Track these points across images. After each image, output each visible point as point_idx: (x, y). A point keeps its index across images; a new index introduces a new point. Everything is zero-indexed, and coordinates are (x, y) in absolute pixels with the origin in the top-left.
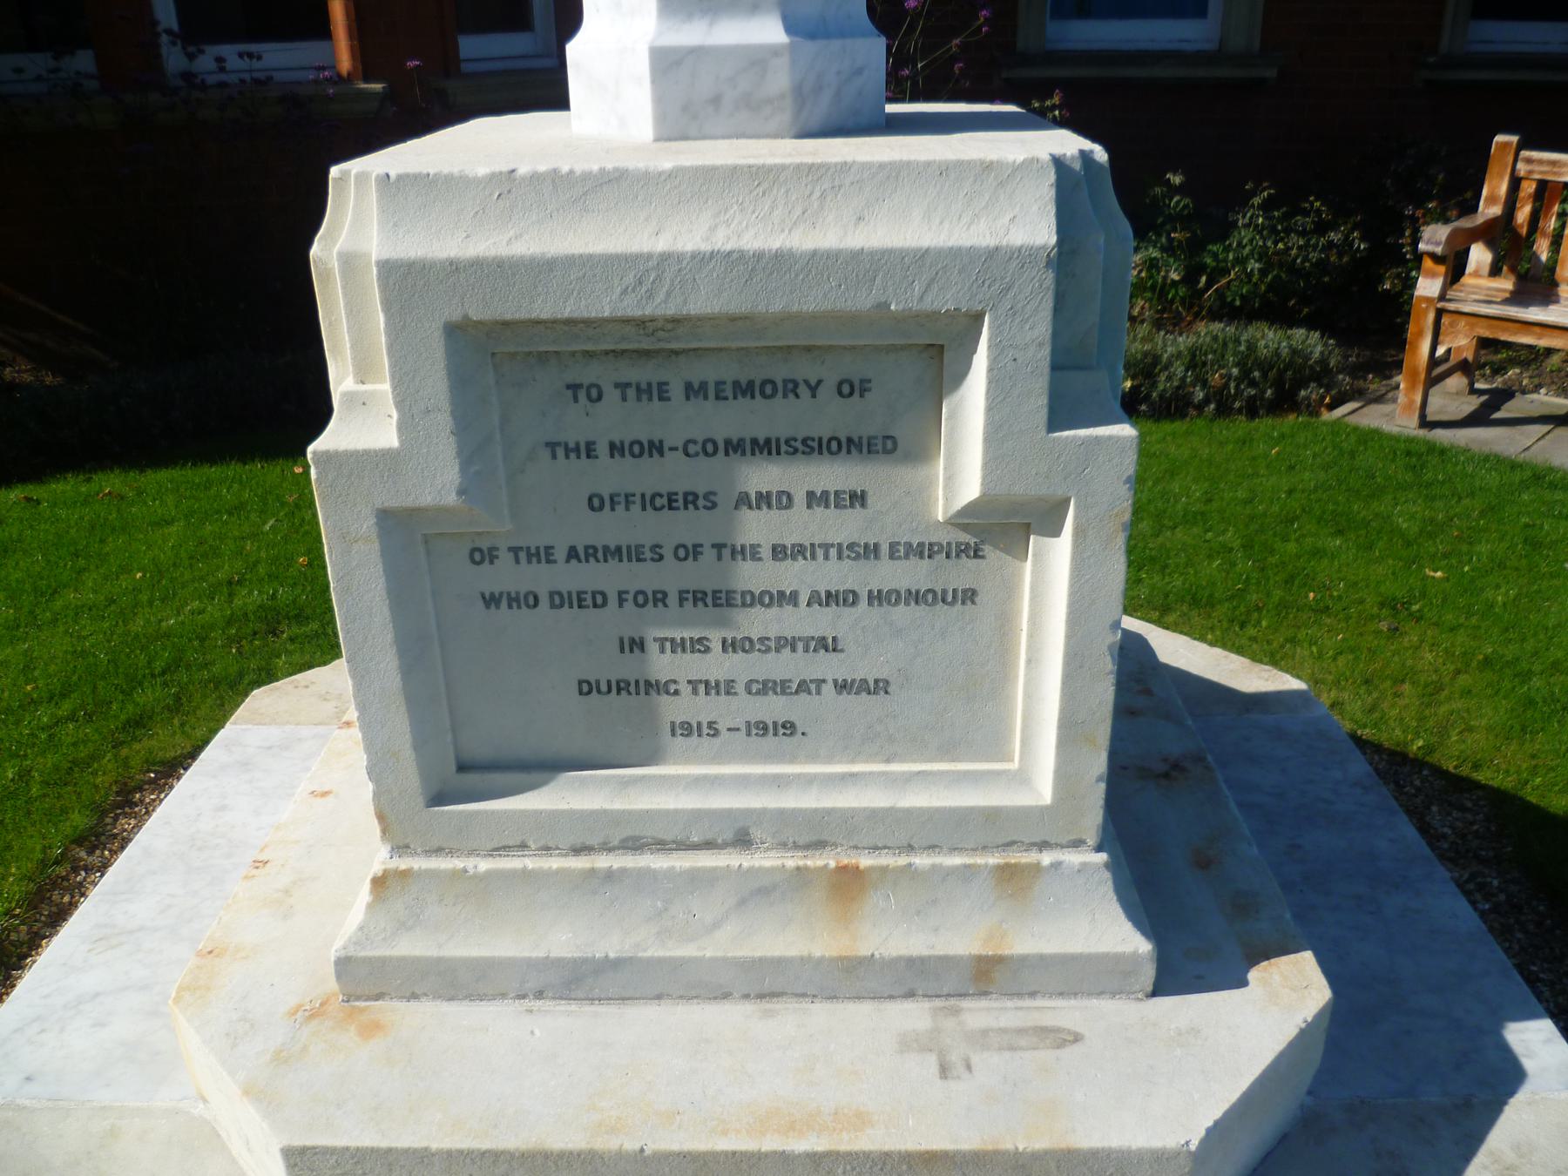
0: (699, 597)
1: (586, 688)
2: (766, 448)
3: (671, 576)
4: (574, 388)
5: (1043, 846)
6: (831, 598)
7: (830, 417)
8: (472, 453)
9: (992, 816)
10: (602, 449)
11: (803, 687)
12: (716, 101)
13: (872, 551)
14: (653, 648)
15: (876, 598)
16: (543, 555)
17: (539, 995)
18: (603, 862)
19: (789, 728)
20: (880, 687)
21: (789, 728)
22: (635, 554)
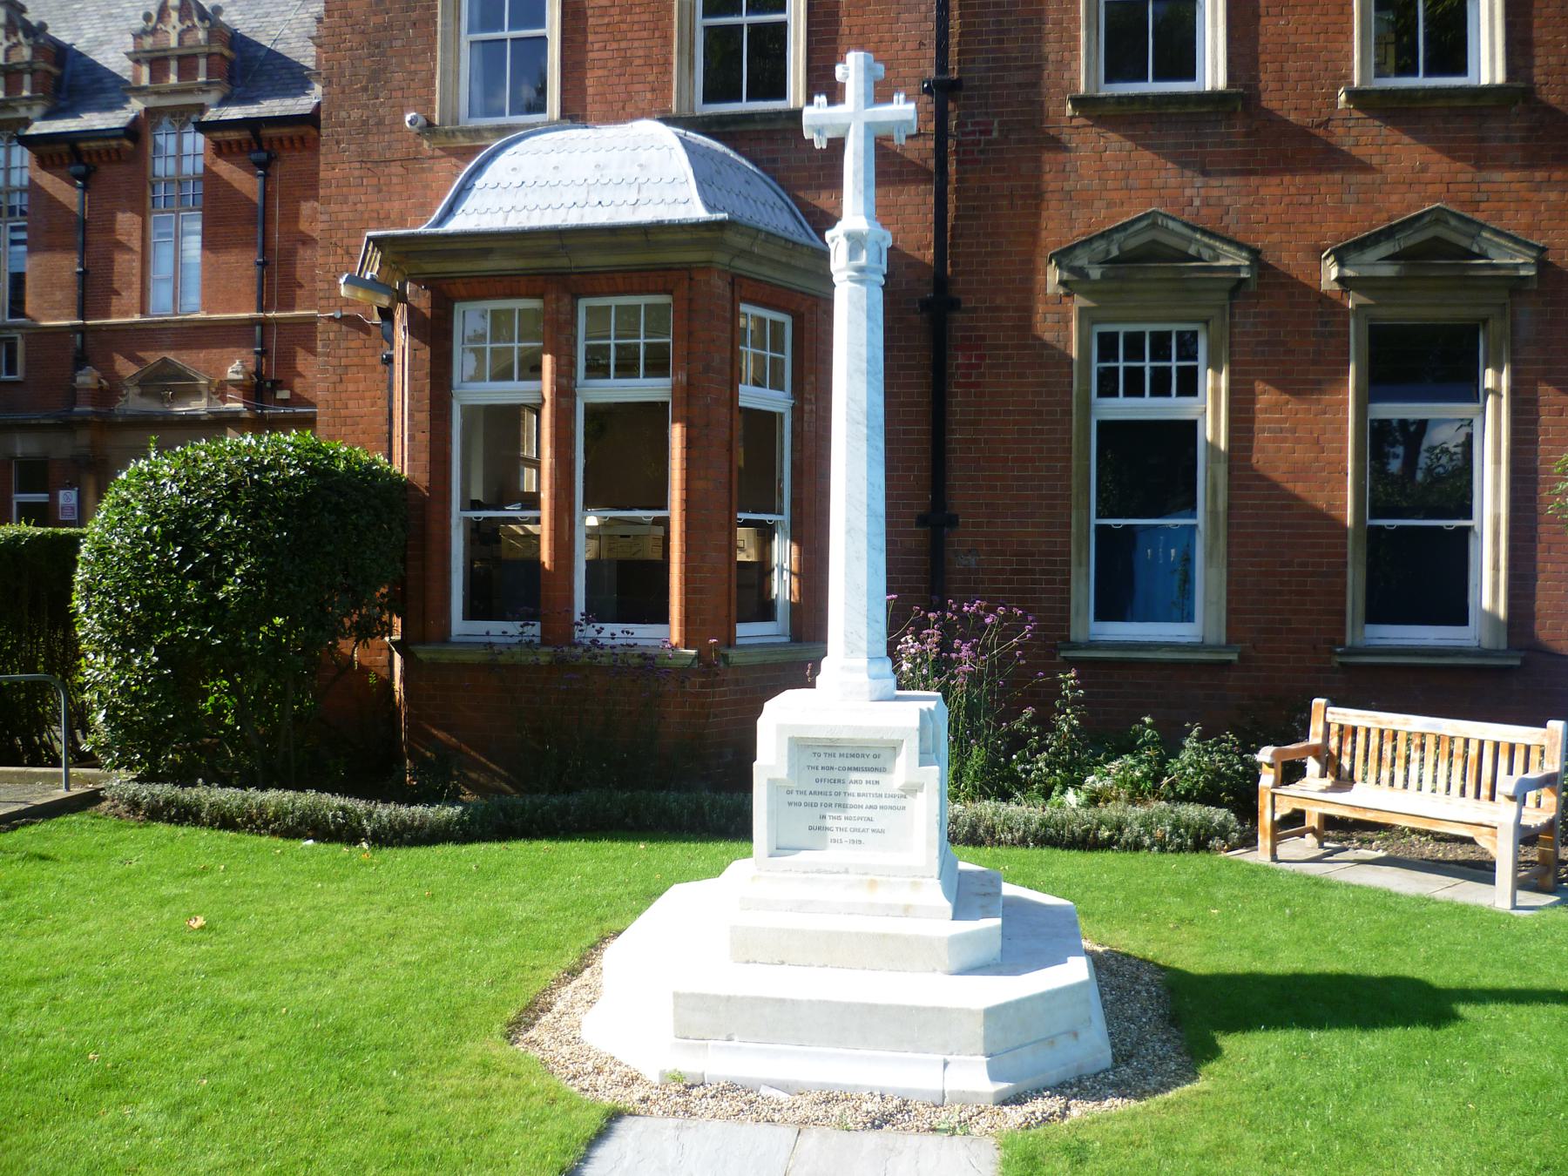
0: (840, 805)
1: (811, 828)
2: (856, 769)
3: (833, 800)
5: (923, 877)
6: (871, 807)
7: (871, 763)
8: (791, 767)
11: (863, 831)
15: (882, 807)
16: (804, 793)
17: (791, 910)
18: (810, 875)
20: (882, 831)
22: (825, 794)
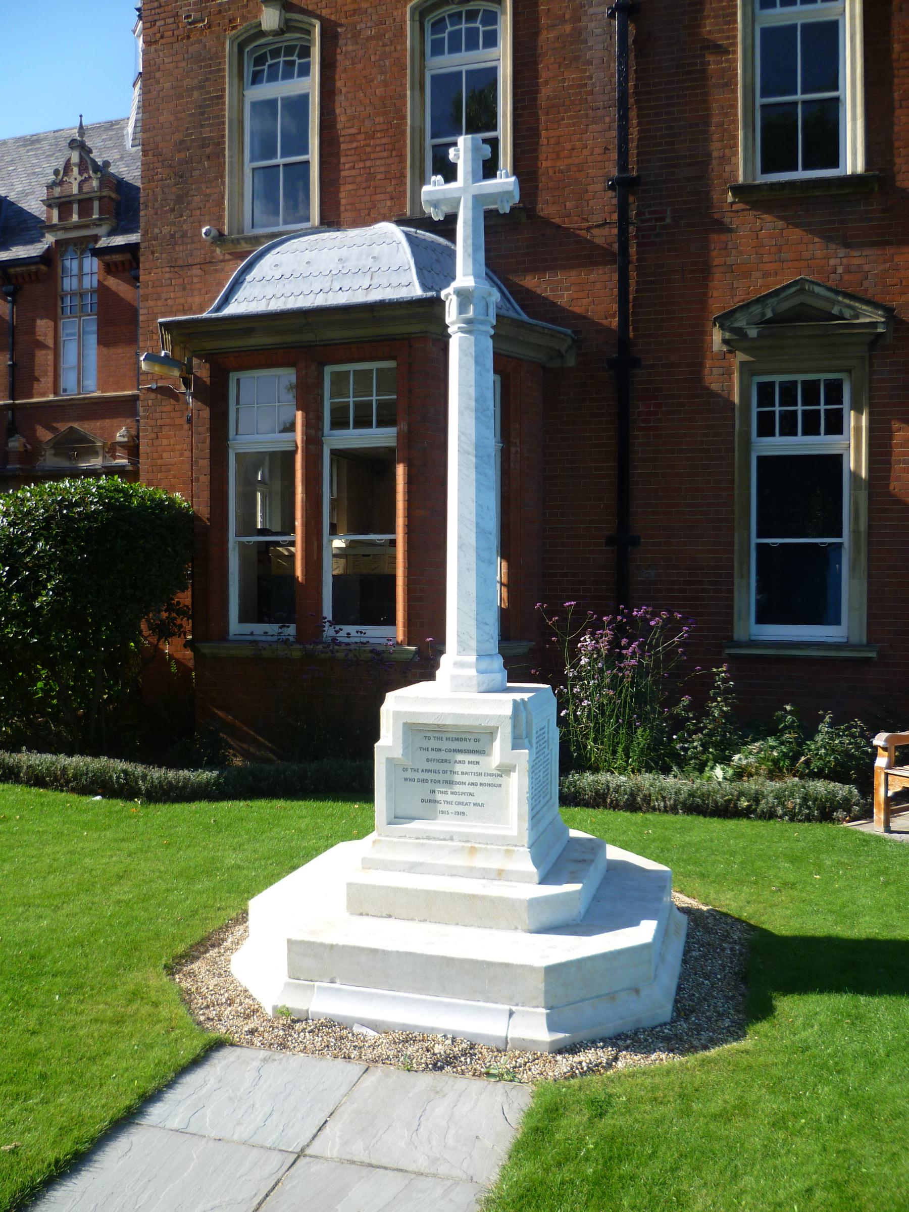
0: (446, 782)
1: (423, 801)
2: (460, 751)
3: (441, 777)
4: (426, 737)
5: (516, 846)
6: (472, 784)
7: (472, 746)
8: (405, 748)
9: (504, 837)
10: (430, 749)
11: (466, 804)
12: (462, 685)
13: (480, 774)
14: (437, 792)
15: (481, 784)
16: (416, 770)
17: (404, 871)
18: (421, 841)
19: (463, 813)
20: (482, 805)
21: (463, 813)
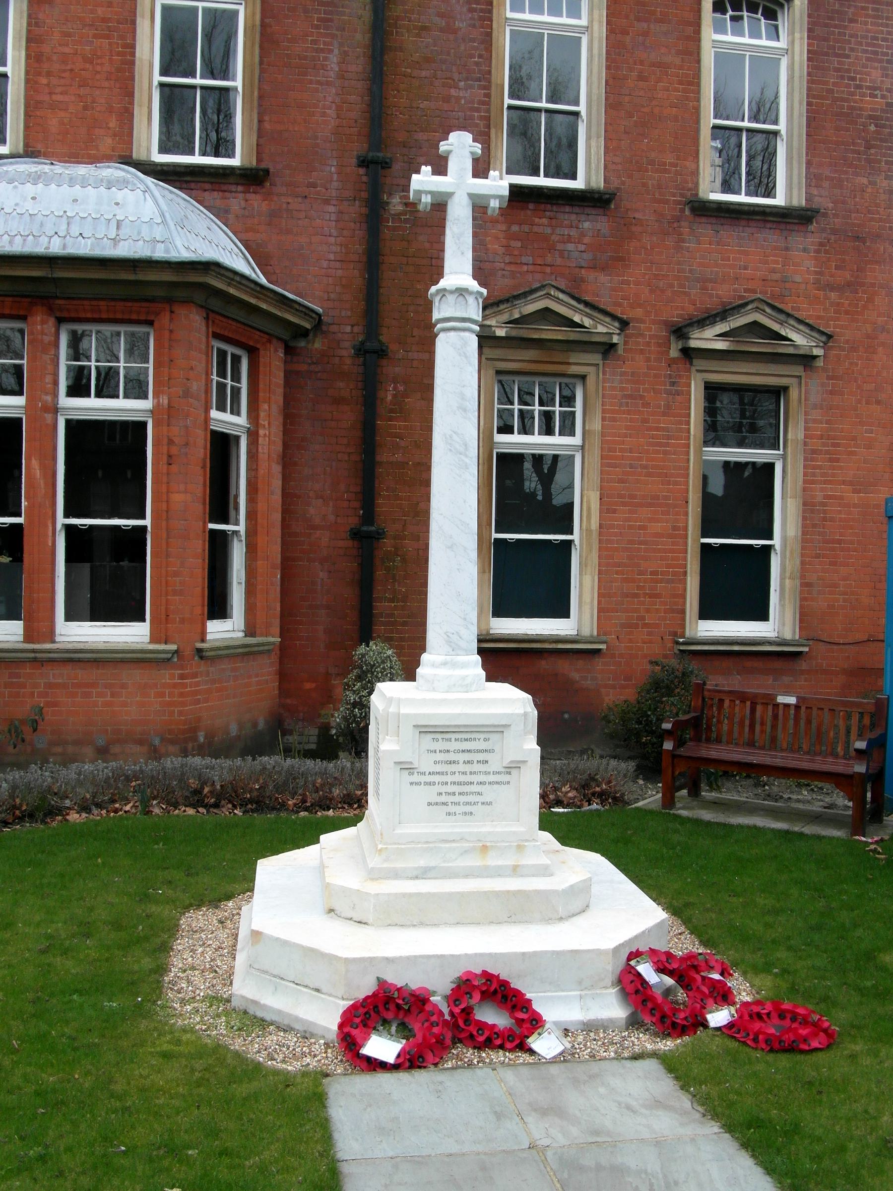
1: (429, 804)
4: (433, 739)
10: (438, 751)
12: (454, 685)
15: (490, 783)
20: (490, 803)
22: (442, 773)
